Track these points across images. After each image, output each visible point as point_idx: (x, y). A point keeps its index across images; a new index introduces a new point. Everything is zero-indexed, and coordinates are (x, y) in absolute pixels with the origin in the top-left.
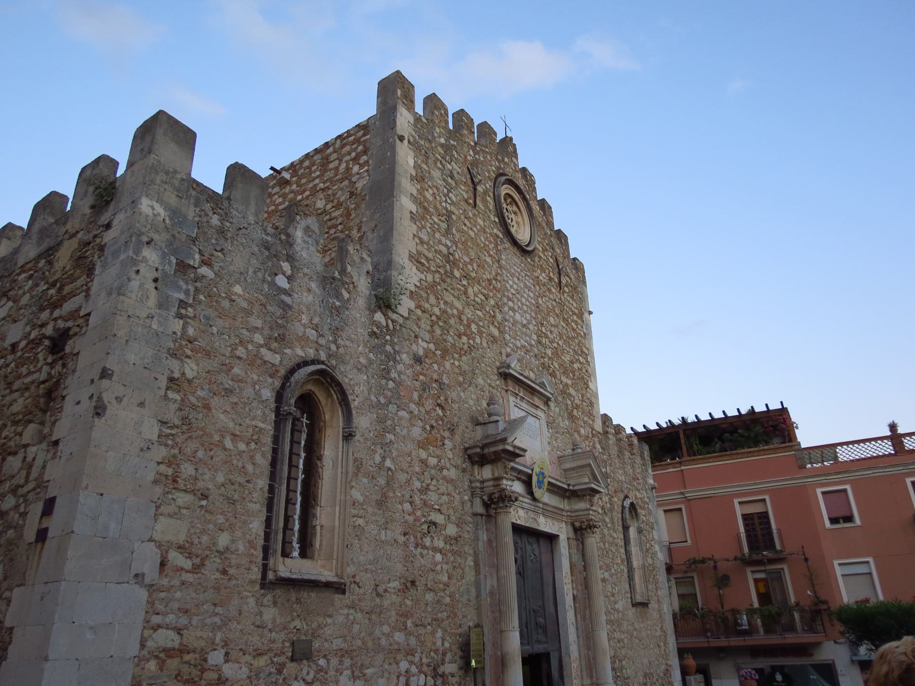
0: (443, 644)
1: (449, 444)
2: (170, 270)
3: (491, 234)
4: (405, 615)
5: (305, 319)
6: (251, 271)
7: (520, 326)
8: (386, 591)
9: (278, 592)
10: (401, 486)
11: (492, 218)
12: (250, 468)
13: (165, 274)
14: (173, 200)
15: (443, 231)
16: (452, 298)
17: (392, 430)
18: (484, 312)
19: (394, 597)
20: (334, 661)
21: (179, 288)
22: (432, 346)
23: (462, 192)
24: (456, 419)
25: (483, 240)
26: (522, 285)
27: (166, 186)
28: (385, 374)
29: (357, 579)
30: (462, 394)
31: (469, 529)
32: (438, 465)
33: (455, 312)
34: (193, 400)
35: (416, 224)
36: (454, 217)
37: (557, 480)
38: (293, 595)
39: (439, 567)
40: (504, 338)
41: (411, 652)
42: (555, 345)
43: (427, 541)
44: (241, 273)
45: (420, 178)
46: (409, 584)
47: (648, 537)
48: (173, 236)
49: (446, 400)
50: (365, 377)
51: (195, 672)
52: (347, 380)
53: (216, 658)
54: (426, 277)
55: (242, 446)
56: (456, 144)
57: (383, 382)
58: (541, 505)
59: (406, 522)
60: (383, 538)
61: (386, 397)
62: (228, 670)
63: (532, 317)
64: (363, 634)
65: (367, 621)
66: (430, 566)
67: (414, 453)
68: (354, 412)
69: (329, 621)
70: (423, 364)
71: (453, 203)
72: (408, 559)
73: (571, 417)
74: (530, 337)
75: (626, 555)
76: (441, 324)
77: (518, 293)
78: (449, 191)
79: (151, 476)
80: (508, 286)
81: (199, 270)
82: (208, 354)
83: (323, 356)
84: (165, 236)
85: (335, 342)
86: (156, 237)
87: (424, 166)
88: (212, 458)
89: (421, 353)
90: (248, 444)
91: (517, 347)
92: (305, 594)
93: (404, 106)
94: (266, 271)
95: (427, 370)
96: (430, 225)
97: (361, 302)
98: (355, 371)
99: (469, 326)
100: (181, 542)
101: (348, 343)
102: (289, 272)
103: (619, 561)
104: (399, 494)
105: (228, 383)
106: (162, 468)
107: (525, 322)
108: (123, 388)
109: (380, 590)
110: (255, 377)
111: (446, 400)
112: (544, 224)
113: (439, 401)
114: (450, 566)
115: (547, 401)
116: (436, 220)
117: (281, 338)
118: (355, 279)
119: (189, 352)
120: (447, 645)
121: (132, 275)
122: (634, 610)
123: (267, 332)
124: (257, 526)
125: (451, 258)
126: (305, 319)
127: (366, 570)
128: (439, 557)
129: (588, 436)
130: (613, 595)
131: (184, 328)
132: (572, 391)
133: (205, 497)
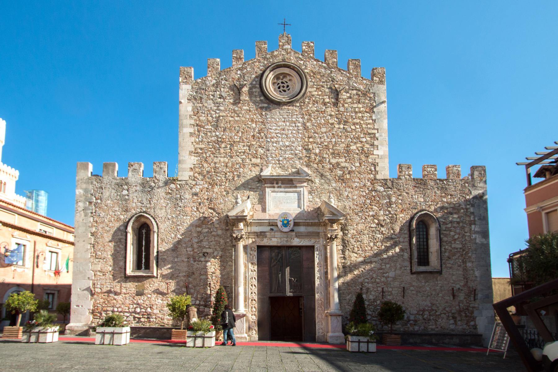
5: (135, 201)
8: (177, 276)
11: (258, 99)
19: (182, 278)
25: (248, 117)
26: (288, 124)
32: (208, 231)
42: (326, 144)
43: (203, 259)
46: (190, 274)
47: (458, 231)
50: (165, 210)
59: (188, 254)
60: (176, 260)
67: (193, 230)
68: (159, 224)
72: (189, 266)
73: (341, 179)
80: (272, 131)
83: (144, 209)
87: (200, 105)
89: (198, 190)
107: (287, 144)
113: (210, 206)
118: (158, 176)
122: (415, 276)
126: (135, 201)
129: (365, 185)
130: (382, 269)
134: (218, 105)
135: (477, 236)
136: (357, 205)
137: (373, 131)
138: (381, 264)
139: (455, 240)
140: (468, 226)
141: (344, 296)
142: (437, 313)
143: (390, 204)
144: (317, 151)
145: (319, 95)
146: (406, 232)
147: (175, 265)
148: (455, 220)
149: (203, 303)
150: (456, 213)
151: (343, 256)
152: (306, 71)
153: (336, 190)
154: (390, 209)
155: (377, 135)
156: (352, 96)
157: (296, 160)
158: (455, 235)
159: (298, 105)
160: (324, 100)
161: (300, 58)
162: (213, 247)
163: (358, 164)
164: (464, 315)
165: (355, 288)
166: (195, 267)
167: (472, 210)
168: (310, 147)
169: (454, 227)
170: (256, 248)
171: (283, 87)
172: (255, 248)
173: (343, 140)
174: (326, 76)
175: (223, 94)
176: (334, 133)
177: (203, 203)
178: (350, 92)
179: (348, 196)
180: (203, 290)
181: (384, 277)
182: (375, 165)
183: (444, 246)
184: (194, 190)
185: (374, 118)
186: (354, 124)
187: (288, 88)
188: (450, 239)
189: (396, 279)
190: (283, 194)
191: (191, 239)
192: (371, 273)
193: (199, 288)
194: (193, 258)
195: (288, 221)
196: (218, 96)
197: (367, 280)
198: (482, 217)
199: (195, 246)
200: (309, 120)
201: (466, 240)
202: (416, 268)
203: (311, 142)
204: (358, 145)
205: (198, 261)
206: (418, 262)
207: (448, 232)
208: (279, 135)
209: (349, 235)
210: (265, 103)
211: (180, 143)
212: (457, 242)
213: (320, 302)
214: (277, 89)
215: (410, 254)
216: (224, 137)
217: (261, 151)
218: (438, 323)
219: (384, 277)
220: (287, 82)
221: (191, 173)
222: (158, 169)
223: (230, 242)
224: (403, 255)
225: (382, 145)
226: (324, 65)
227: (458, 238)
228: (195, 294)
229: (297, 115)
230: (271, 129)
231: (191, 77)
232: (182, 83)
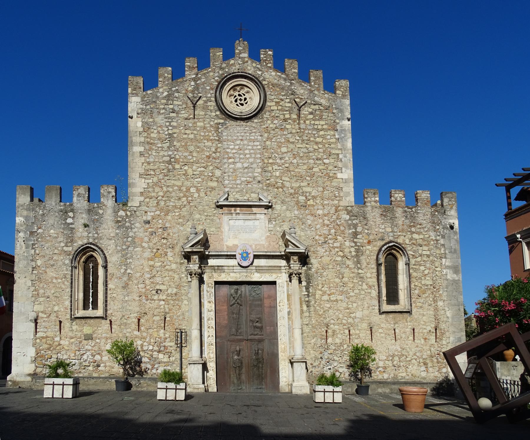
0: (165, 335)
1: (170, 254)
2: (28, 236)
3: (211, 126)
6: (56, 222)
7: (240, 170)
8: (128, 317)
9: (77, 320)
10: (137, 279)
12: (63, 286)
13: (26, 238)
15: (166, 148)
16: (173, 182)
17: (132, 257)
18: (203, 177)
20: (103, 340)
21: (31, 240)
22: (158, 213)
23: (182, 115)
24: (175, 242)
25: (202, 134)
26: (246, 142)
29: (113, 315)
30: (182, 228)
31: (185, 289)
32: (161, 265)
33: (176, 188)
34: (40, 271)
35: (144, 156)
36: (175, 135)
37: (266, 252)
38: (83, 321)
39: (162, 307)
40: (223, 184)
42: (287, 165)
43: (156, 297)
44: (52, 225)
45: (147, 127)
46: (143, 315)
47: (428, 265)
48: (27, 225)
49: (169, 234)
50: (114, 241)
52: (103, 246)
54: (153, 180)
55: (60, 281)
56: (177, 88)
57: (125, 240)
58: (254, 268)
60: (127, 298)
61: (126, 246)
63: (255, 158)
64: (117, 332)
65: (118, 328)
66: (156, 306)
67: (145, 264)
68: (108, 257)
69: (100, 328)
70: (151, 223)
71: (174, 127)
74: (253, 173)
76: (164, 199)
77: (241, 150)
78: (170, 122)
79: (31, 295)
80: (228, 150)
81: (38, 232)
82: (44, 257)
83: (91, 240)
84: (25, 226)
85: (97, 233)
86: (22, 228)
87: (151, 120)
89: (149, 218)
90: (62, 279)
91: (238, 184)
92: (89, 321)
93: (133, 95)
94: (62, 220)
95: (154, 225)
96: (155, 151)
97: (110, 211)
98: (108, 240)
99: (188, 190)
100: (42, 311)
101: (103, 231)
102: (72, 216)
103: (365, 287)
104: (135, 282)
105: (52, 262)
106: (34, 292)
107: (246, 165)
109: (126, 317)
110: (62, 258)
111: (169, 234)
113: (163, 237)
115: (267, 207)
116: (160, 145)
118: (105, 203)
119: (37, 258)
120: (167, 336)
122: (383, 316)
123: (65, 241)
124: (68, 303)
125: (173, 160)
126: (81, 230)
127: (118, 311)
128: (162, 303)
130: (348, 309)
131: (35, 251)
132: (308, 189)
133: (48, 297)
135: (448, 271)
136: (320, 235)
137: (337, 152)
138: (347, 303)
139: (425, 275)
140: (439, 260)
141: (309, 339)
143: (355, 235)
144: (278, 174)
145: (279, 110)
146: (374, 266)
147: (126, 304)
148: (424, 253)
149: (157, 349)
150: (425, 245)
151: (306, 293)
152: (264, 83)
153: (298, 218)
154: (355, 240)
155: (341, 156)
156: (314, 112)
157: (254, 184)
158: (425, 270)
159: (256, 121)
160: (284, 116)
161: (258, 68)
162: (166, 283)
163: (321, 189)
165: (320, 330)
166: (147, 307)
167: (442, 241)
168: (270, 168)
169: (424, 261)
171: (241, 100)
172: (212, 284)
173: (306, 162)
174: (286, 88)
175: (176, 108)
176: (296, 153)
177: (155, 233)
178: (313, 107)
179: (310, 225)
180: (156, 333)
181: (350, 317)
182: (340, 189)
183: (414, 282)
184: (145, 218)
185: (337, 136)
186: (317, 143)
187: (246, 102)
188: (419, 275)
189: (364, 320)
190: (241, 223)
191: (143, 274)
192: (337, 314)
193: (152, 330)
194: (145, 296)
195: (248, 254)
196: (171, 111)
197: (332, 321)
198: (453, 250)
199: (147, 282)
200: (268, 139)
201: (437, 275)
202: (386, 307)
203: (270, 163)
204: (321, 167)
206: (387, 300)
207: (417, 267)
208: (237, 156)
209: (313, 270)
210: (221, 119)
211: (130, 164)
212: (427, 278)
213: (283, 346)
214: (234, 102)
215: (377, 291)
216: (177, 157)
217: (218, 173)
219: (350, 317)
220: (244, 95)
221: (142, 199)
222: (105, 194)
223: (185, 278)
224: (370, 293)
225: (346, 167)
226: (283, 76)
227: (429, 273)
228: (148, 338)
229: (254, 132)
230: (228, 148)
231: (140, 88)
232: (130, 95)
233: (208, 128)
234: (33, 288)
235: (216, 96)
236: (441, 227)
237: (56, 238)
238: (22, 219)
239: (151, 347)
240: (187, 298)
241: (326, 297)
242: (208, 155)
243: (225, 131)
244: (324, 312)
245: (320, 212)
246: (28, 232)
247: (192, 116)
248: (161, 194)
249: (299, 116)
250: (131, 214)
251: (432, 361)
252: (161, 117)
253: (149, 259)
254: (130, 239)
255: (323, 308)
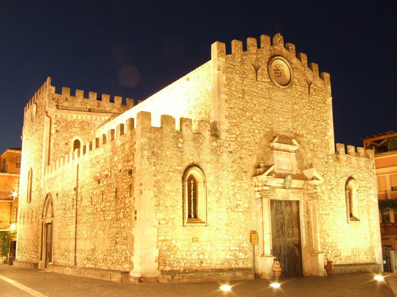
2: (150, 155)
4: (228, 231)
5: (188, 154)
6: (171, 146)
14: (148, 135)
27: (146, 133)
28: (218, 161)
30: (251, 159)
34: (160, 185)
41: (230, 240)
43: (236, 210)
44: (168, 148)
48: (150, 145)
51: (170, 245)
53: (174, 242)
55: (174, 194)
62: (177, 244)
75: (346, 203)
78: (243, 81)
80: (276, 108)
84: (148, 146)
88: (167, 198)
89: (232, 150)
98: (207, 164)
99: (254, 132)
105: (168, 178)
108: (145, 187)
110: (176, 175)
112: (300, 67)
114: (246, 217)
117: (182, 162)
120: (244, 239)
121: (142, 159)
123: (177, 161)
125: (245, 109)
126: (188, 154)
128: (240, 214)
132: (314, 141)
134: (243, 79)
142: (360, 251)
154: (336, 176)
155: (328, 121)
164: (370, 251)
170: (270, 201)
171: (278, 73)
175: (246, 71)
184: (229, 149)
185: (326, 108)
205: (234, 212)
216: (247, 107)
218: (360, 257)
223: (254, 196)
233: (264, 90)
234: (155, 199)
235: (268, 68)
236: (369, 170)
237: (171, 158)
238: (146, 140)
239: (235, 248)
240: (255, 211)
241: (324, 212)
242: (264, 108)
243: (273, 94)
244: (324, 222)
245: (320, 156)
246: (151, 152)
247: (255, 79)
248: (238, 133)
249: (309, 91)
250: (220, 145)
251: (369, 252)
252: (237, 75)
253: (232, 181)
254: (220, 164)
255: (323, 219)
